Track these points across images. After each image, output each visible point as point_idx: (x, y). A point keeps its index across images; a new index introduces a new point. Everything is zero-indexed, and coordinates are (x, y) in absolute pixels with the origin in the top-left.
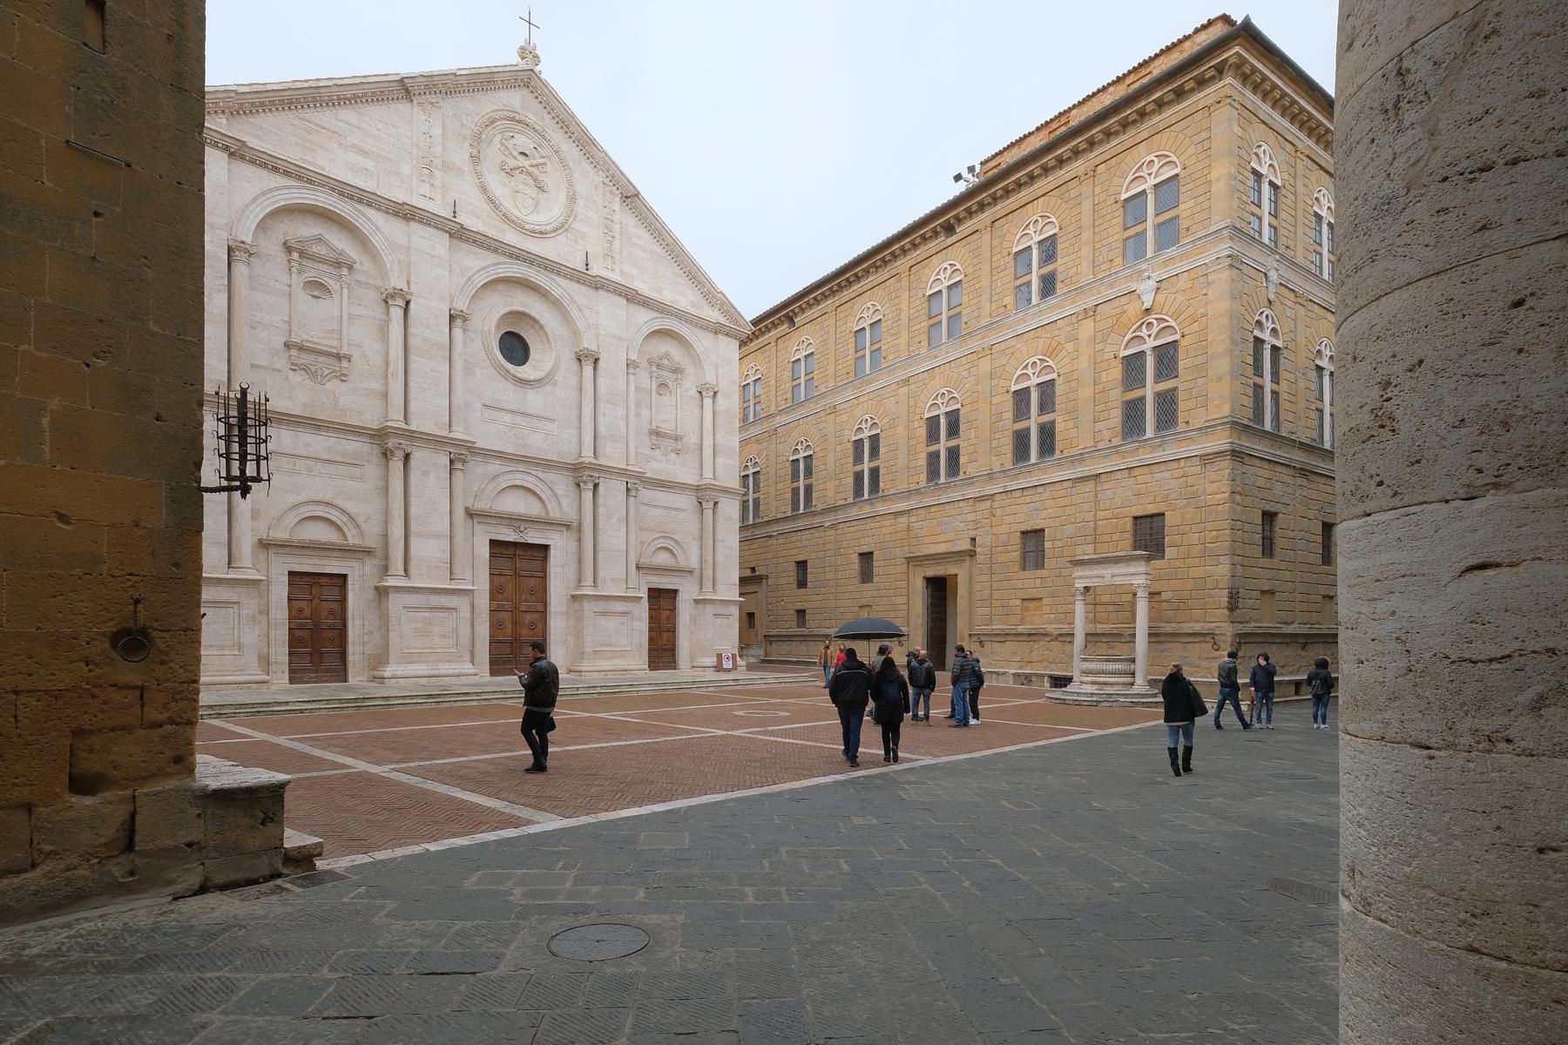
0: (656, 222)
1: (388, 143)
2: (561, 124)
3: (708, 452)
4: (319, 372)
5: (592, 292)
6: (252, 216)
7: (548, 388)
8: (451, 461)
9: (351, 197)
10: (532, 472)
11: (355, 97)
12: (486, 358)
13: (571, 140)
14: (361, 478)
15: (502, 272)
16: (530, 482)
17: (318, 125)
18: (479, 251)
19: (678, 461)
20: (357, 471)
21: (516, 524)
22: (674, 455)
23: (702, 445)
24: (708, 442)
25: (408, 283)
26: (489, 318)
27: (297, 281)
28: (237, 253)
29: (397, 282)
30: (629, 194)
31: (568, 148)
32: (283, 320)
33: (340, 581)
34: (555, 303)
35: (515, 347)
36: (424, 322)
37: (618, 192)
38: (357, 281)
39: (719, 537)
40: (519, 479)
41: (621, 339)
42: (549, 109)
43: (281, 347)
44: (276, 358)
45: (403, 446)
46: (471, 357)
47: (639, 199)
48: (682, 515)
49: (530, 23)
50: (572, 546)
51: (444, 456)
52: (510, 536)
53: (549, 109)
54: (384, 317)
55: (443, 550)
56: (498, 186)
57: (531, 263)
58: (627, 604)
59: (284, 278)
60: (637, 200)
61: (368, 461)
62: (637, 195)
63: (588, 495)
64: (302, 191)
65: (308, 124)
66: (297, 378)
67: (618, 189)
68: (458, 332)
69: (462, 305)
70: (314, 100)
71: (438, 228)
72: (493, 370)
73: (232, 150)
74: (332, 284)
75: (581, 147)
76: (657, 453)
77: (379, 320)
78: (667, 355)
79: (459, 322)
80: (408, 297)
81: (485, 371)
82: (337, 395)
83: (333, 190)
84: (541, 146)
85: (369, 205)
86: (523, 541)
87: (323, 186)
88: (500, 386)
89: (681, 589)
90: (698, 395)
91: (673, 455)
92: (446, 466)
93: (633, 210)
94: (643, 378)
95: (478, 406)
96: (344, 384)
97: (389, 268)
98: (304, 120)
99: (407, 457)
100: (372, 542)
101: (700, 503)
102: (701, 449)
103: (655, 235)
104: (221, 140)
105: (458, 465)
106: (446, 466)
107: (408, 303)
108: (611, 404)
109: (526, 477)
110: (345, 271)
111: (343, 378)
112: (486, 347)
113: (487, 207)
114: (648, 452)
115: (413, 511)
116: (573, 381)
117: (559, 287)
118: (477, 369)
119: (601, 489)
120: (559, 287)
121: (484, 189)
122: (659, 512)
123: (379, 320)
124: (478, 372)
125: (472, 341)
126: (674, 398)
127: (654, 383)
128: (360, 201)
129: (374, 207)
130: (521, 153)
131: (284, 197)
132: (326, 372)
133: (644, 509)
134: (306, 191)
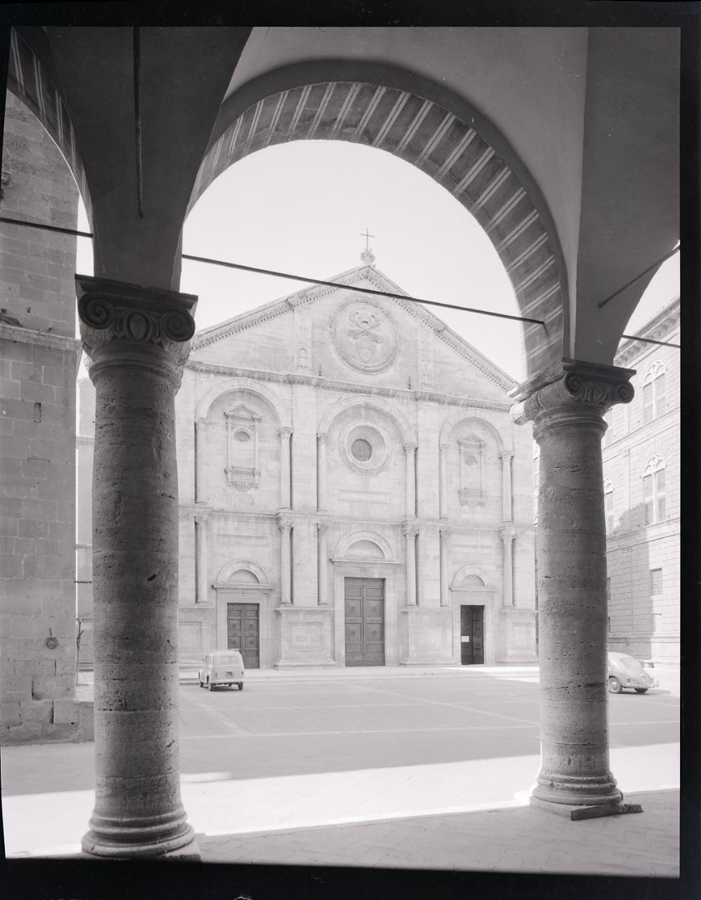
3: (508, 502)
7: (383, 474)
20: (265, 542)
23: (502, 497)
24: (507, 494)
25: (292, 422)
26: (345, 435)
27: (231, 433)
29: (285, 423)
33: (255, 607)
35: (363, 447)
48: (486, 551)
62: (446, 328)
63: (411, 543)
67: (431, 327)
68: (323, 447)
69: (324, 429)
74: (249, 431)
76: (466, 507)
79: (323, 440)
80: (292, 431)
90: (498, 461)
91: (479, 508)
94: (452, 455)
101: (502, 540)
102: (502, 500)
107: (292, 435)
111: (253, 485)
112: (343, 453)
117: (390, 405)
119: (421, 538)
120: (390, 405)
127: (462, 456)
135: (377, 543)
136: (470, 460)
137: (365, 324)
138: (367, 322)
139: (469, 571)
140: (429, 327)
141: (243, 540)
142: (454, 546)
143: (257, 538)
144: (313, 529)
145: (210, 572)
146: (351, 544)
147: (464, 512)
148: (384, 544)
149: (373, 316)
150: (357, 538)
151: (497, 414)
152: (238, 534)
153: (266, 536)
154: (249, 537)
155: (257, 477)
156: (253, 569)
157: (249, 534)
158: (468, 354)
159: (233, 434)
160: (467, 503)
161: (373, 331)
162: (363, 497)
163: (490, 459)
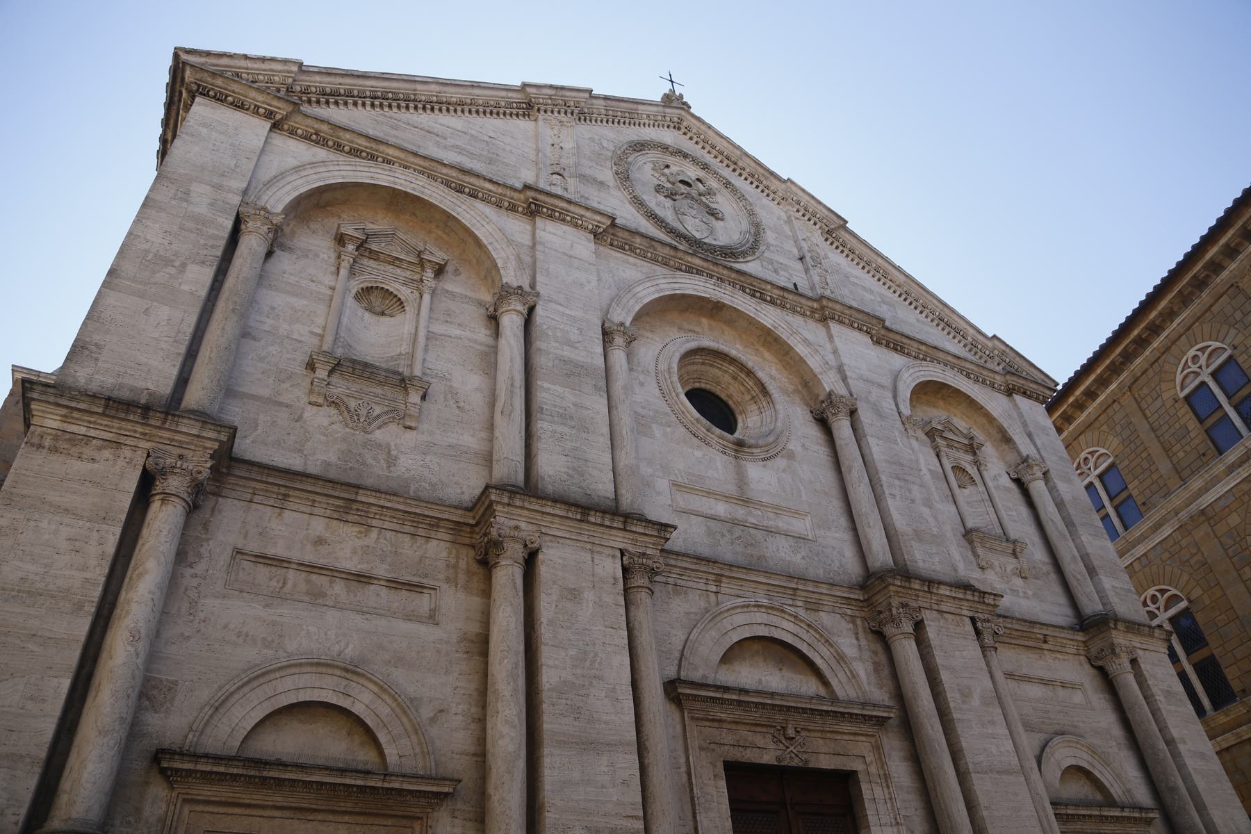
0: (875, 257)
2: (726, 162)
4: (363, 412)
6: (289, 187)
8: (626, 570)
11: (461, 103)
12: (668, 410)
14: (432, 618)
15: (680, 288)
16: (786, 630)
18: (639, 262)
20: (423, 603)
21: (779, 718)
28: (250, 224)
30: (833, 226)
32: (312, 333)
34: (770, 340)
36: (559, 334)
38: (447, 291)
43: (299, 370)
44: (287, 385)
45: (523, 535)
46: (644, 408)
48: (1078, 697)
49: (671, 81)
50: (900, 770)
51: (610, 559)
52: (767, 753)
53: (708, 148)
54: (490, 341)
55: (624, 782)
59: (329, 280)
61: (448, 580)
64: (372, 170)
66: (320, 418)
68: (618, 356)
71: (576, 226)
72: (683, 430)
73: (278, 117)
74: (404, 292)
75: (756, 183)
77: (481, 344)
79: (619, 340)
82: (394, 453)
85: (473, 195)
86: (796, 762)
88: (698, 454)
91: (1018, 582)
92: (615, 579)
93: (841, 248)
95: (663, 484)
96: (410, 435)
97: (499, 265)
99: (530, 560)
100: (456, 761)
104: (263, 102)
105: (639, 580)
106: (615, 579)
107: (531, 310)
109: (775, 620)
110: (429, 274)
115: (548, 678)
116: (820, 451)
118: (654, 426)
119: (931, 632)
122: (1035, 691)
123: (481, 344)
124: (657, 430)
125: (642, 384)
126: (982, 488)
131: (343, 173)
132: (378, 410)
135: (804, 648)
140: (812, 222)
141: (339, 588)
143: (394, 584)
144: (611, 567)
148: (825, 651)
149: (698, 180)
150: (744, 624)
152: (322, 562)
153: (432, 583)
154: (363, 579)
155: (414, 397)
156: (362, 702)
157: (361, 567)
159: (356, 285)
162: (740, 512)
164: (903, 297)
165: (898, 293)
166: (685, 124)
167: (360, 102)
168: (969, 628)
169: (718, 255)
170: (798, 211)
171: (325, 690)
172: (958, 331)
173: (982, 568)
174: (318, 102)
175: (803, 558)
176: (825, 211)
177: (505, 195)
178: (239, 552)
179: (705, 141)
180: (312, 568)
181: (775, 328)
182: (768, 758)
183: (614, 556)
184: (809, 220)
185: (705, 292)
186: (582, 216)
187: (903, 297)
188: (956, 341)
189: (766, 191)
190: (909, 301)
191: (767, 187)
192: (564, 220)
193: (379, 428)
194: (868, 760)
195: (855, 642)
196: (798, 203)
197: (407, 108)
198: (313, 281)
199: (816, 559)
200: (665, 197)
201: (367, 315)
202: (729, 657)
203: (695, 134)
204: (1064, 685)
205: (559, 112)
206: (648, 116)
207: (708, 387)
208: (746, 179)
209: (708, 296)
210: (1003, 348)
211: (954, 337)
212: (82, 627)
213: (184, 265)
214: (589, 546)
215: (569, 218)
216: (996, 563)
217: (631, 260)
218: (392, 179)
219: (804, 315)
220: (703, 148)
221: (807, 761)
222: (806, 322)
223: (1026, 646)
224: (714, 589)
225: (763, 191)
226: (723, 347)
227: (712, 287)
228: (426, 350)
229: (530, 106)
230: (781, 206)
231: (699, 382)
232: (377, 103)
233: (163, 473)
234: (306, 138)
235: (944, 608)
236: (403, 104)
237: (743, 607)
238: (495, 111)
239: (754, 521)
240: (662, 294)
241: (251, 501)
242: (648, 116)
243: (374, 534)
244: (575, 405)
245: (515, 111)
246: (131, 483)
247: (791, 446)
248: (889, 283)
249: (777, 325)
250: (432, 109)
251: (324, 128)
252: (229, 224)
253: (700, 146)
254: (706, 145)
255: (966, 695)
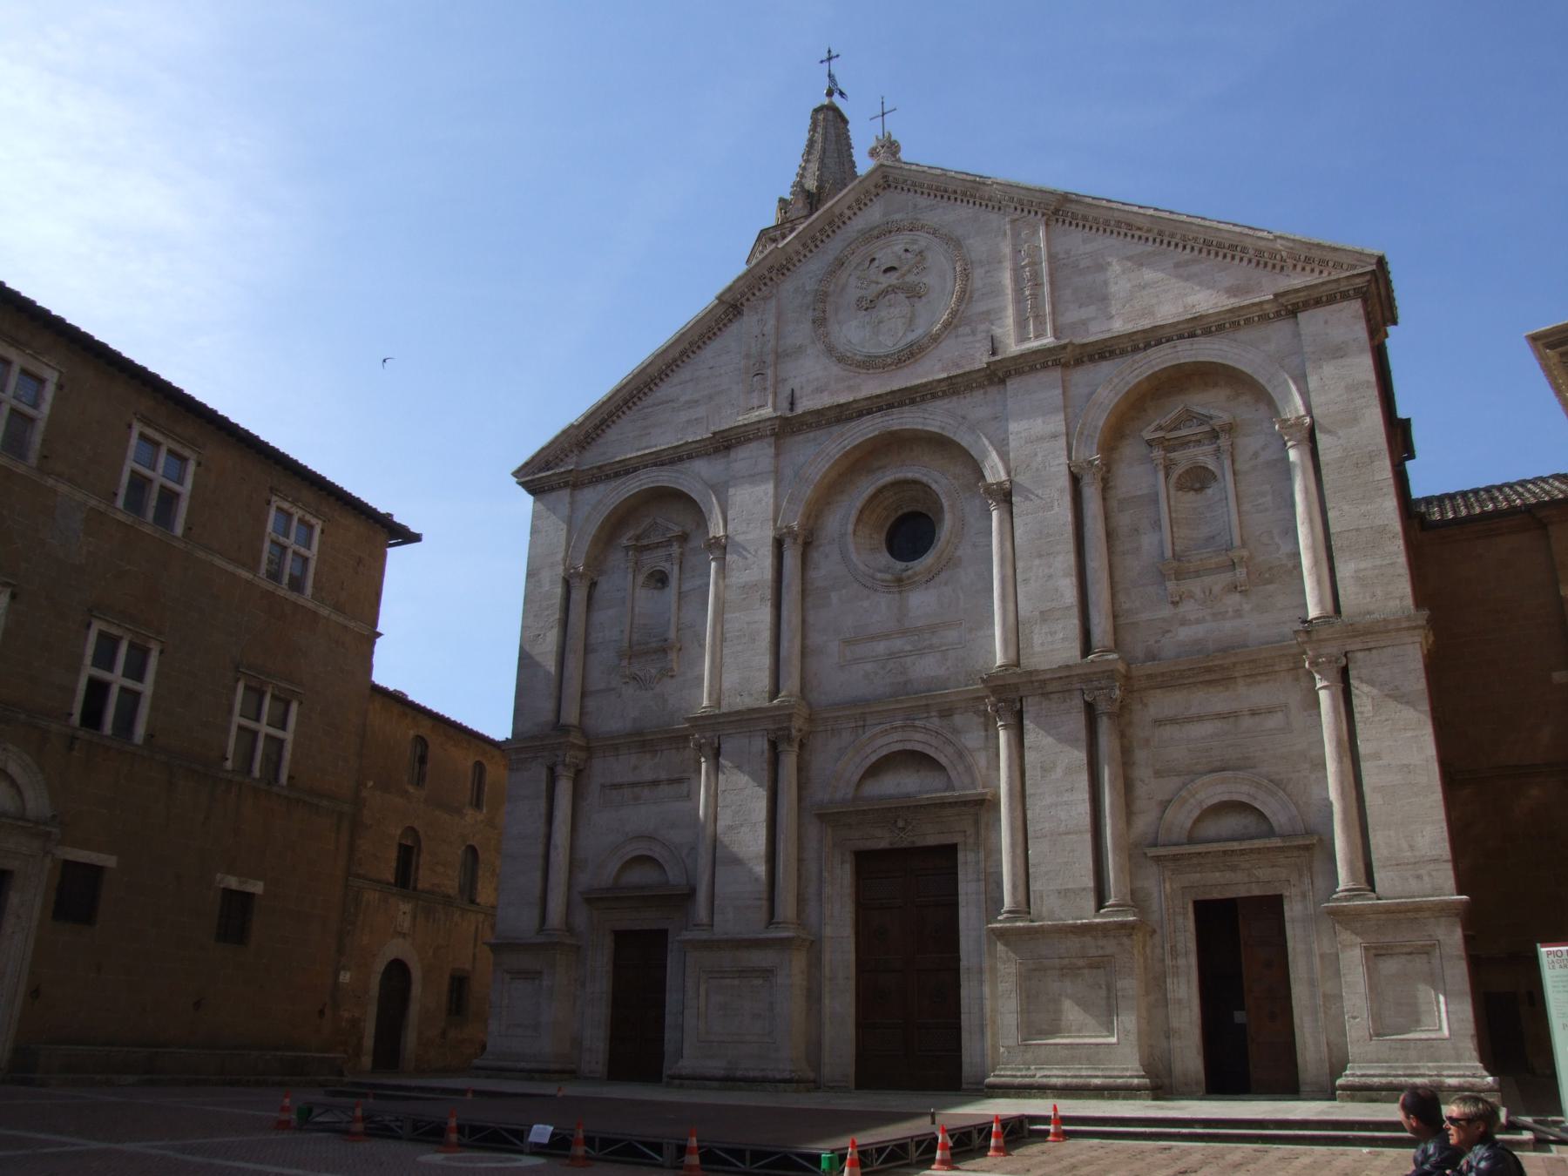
1: (721, 375)
2: (939, 194)
5: (993, 391)
9: (672, 462)
10: (917, 723)
13: (959, 202)
17: (654, 405)
19: (1247, 607)
22: (1237, 597)
31: (952, 216)
34: (941, 444)
37: (1040, 215)
39: (1363, 748)
40: (893, 742)
41: (1054, 436)
42: (919, 190)
47: (1071, 201)
49: (883, 114)
52: (882, 839)
53: (919, 190)
56: (853, 333)
57: (891, 406)
58: (1101, 943)
60: (1068, 205)
62: (1066, 198)
65: (646, 410)
67: (1036, 213)
70: (647, 385)
76: (1189, 609)
78: (1189, 417)
81: (844, 591)
83: (655, 465)
84: (914, 242)
86: (904, 845)
87: (646, 466)
88: (866, 604)
89: (1286, 893)
92: (763, 752)
98: (644, 408)
103: (1123, 231)
108: (1040, 556)
113: (836, 370)
114: (1166, 611)
121: (830, 350)
124: (834, 597)
125: (827, 556)
128: (681, 459)
129: (697, 456)
130: (886, 271)
133: (1168, 731)
134: (630, 482)
135: (932, 753)
136: (1198, 479)
137: (888, 275)
138: (892, 269)
139: (1213, 791)
140: (1033, 213)
142: (1159, 723)
143: (671, 782)
145: (573, 865)
146: (868, 763)
147: (1184, 622)
149: (906, 251)
151: (1244, 335)
154: (655, 783)
156: (657, 852)
158: (1139, 229)
159: (641, 579)
160: (1191, 596)
161: (910, 278)
163: (1256, 455)
164: (1158, 240)
165: (1151, 239)
166: (890, 178)
167: (621, 413)
168: (1077, 703)
169: (905, 361)
170: (1016, 209)
171: (641, 849)
172: (1233, 247)
173: (1175, 604)
174: (598, 435)
175: (948, 669)
176: (1038, 194)
177: (707, 446)
178: (603, 786)
179: (914, 184)
180: (633, 785)
181: (943, 429)
182: (883, 844)
183: (763, 736)
184: (1029, 212)
185: (874, 430)
186: (758, 429)
187: (1158, 240)
188: (1237, 261)
189: (984, 203)
190: (1165, 242)
191: (981, 198)
192: (750, 439)
193: (657, 683)
194: (968, 833)
195: (983, 733)
196: (1011, 199)
197: (650, 389)
198: (618, 590)
199: (960, 665)
200: (866, 309)
201: (656, 592)
202: (875, 770)
203: (903, 183)
204: (1253, 713)
205: (760, 290)
206: (849, 208)
207: (910, 509)
208: (962, 201)
209: (877, 433)
210: (1291, 245)
211: (1233, 258)
212: (540, 849)
213: (545, 635)
214: (748, 734)
215: (751, 437)
216: (1197, 591)
217: (812, 435)
218: (638, 484)
219: (981, 386)
220: (916, 192)
221: (913, 842)
222: (985, 393)
223: (1207, 681)
224: (862, 723)
225: (981, 205)
226: (900, 475)
227: (881, 420)
228: (679, 609)
229: (734, 306)
230: (1002, 212)
231: (902, 509)
232: (630, 404)
233: (555, 764)
234: (591, 482)
235: (1050, 688)
236: (646, 390)
237: (882, 732)
238: (710, 334)
239: (908, 648)
240: (832, 461)
241: (604, 757)
242: (849, 208)
243: (659, 753)
244: (748, 623)
245: (725, 321)
246: (544, 774)
247: (959, 553)
248: (1138, 233)
249: (943, 425)
250: (667, 375)
251: (595, 471)
252: (559, 590)
253: (912, 193)
254: (916, 188)
255: (1046, 770)
